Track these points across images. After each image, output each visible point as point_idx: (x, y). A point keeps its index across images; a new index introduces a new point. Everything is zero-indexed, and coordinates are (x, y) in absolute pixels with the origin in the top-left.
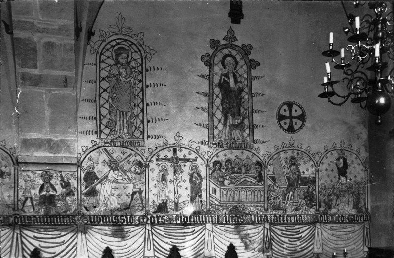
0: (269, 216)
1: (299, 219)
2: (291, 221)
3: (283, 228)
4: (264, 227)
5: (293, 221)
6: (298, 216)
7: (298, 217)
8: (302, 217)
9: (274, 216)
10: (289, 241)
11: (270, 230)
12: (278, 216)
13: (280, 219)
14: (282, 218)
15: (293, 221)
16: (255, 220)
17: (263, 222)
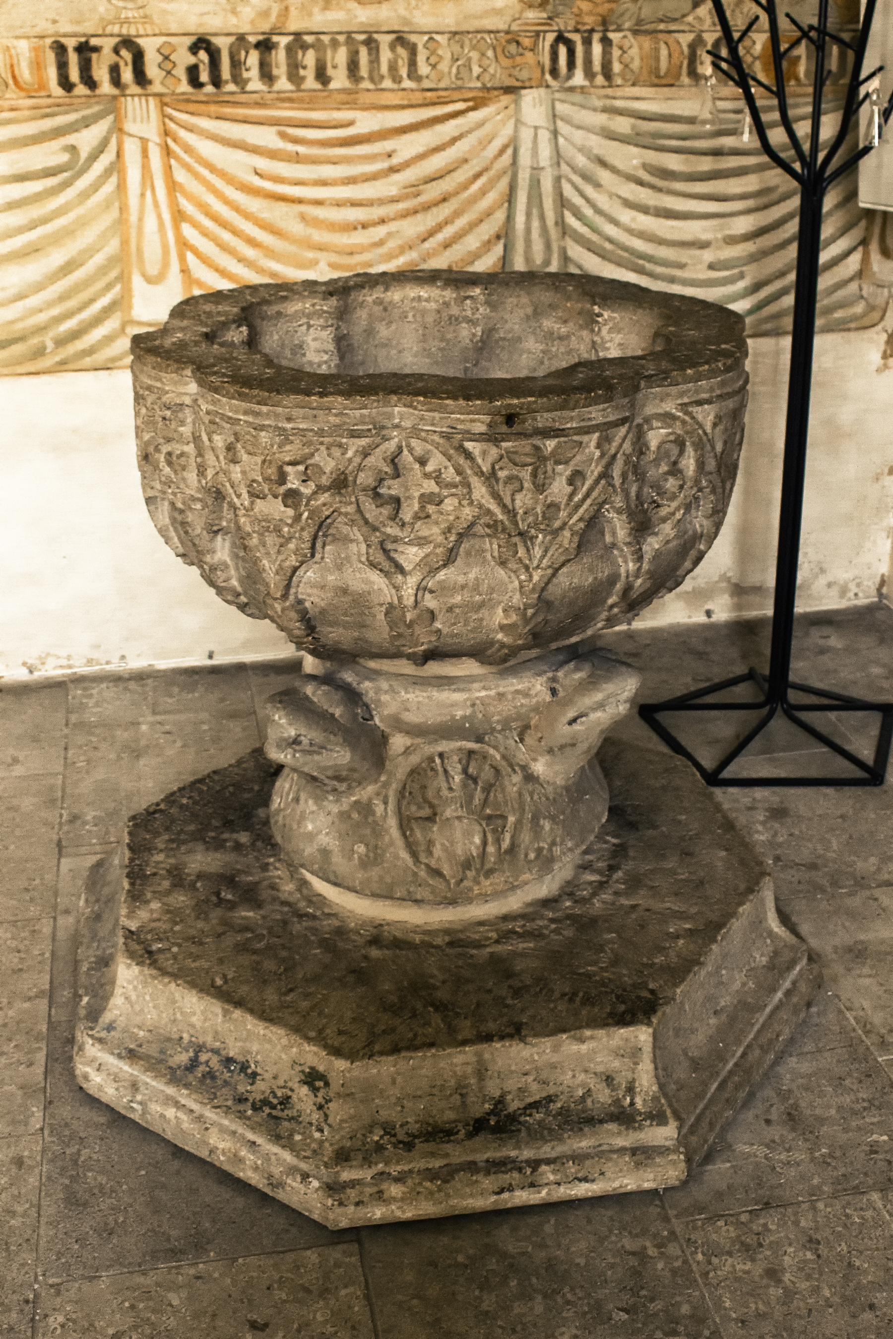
0: (150, 46)
1: (393, 68)
2: (322, 76)
3: (267, 137)
4: (118, 129)
5: (339, 80)
6: (385, 40)
7: (386, 55)
8: (413, 50)
9: (194, 49)
10: (303, 218)
11: (168, 152)
12: (223, 43)
13: (236, 64)
14: (253, 59)
15: (339, 80)
16: (42, 85)
17: (106, 87)
